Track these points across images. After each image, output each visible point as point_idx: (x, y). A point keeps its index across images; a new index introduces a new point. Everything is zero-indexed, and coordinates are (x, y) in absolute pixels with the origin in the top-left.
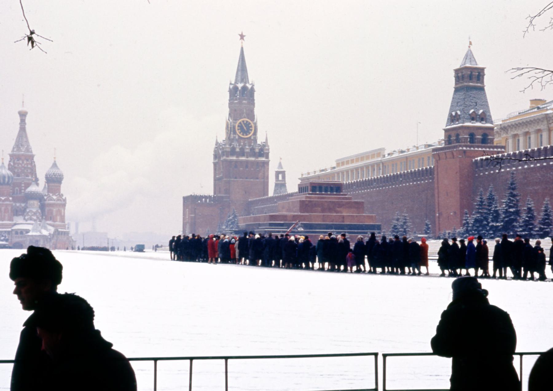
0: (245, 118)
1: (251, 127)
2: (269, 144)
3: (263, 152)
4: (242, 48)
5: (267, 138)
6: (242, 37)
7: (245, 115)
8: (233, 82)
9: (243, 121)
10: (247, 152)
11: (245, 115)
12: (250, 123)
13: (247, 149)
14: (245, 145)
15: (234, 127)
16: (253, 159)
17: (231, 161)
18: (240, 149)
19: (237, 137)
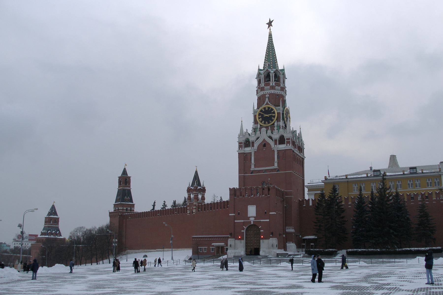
5: (300, 132)
6: (270, 24)
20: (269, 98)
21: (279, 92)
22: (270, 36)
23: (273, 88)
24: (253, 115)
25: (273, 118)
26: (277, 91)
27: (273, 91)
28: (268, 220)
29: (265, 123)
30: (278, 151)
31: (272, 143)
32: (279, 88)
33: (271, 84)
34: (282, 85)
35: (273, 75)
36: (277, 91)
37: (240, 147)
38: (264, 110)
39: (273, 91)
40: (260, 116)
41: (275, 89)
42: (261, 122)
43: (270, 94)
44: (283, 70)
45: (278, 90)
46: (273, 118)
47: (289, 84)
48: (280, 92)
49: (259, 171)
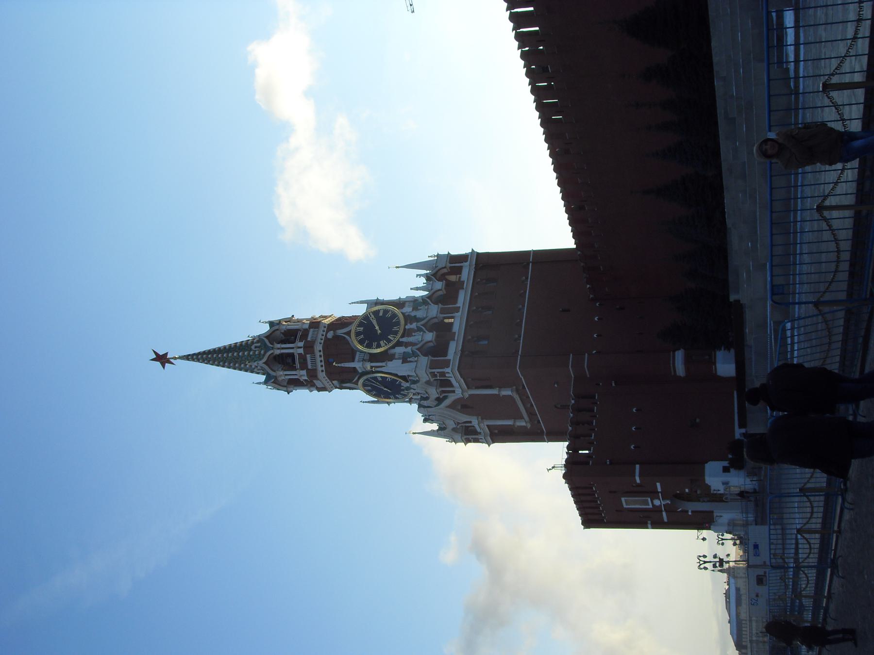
0: (348, 334)
1: (376, 313)
2: (425, 256)
3: (446, 272)
4: (188, 357)
6: (162, 359)
7: (340, 332)
8: (263, 378)
9: (358, 334)
10: (442, 311)
11: (340, 332)
12: (366, 317)
13: (434, 310)
14: (416, 319)
15: (373, 358)
16: (463, 298)
17: (465, 353)
18: (430, 331)
19: (399, 350)
21: (318, 359)
22: (188, 357)
23: (313, 374)
26: (319, 364)
28: (658, 485)
30: (468, 388)
31: (452, 398)
32: (308, 356)
34: (301, 351)
35: (281, 373)
36: (319, 361)
37: (476, 441)
39: (322, 375)
42: (405, 395)
43: (331, 379)
45: (314, 362)
48: (318, 354)
49: (531, 414)
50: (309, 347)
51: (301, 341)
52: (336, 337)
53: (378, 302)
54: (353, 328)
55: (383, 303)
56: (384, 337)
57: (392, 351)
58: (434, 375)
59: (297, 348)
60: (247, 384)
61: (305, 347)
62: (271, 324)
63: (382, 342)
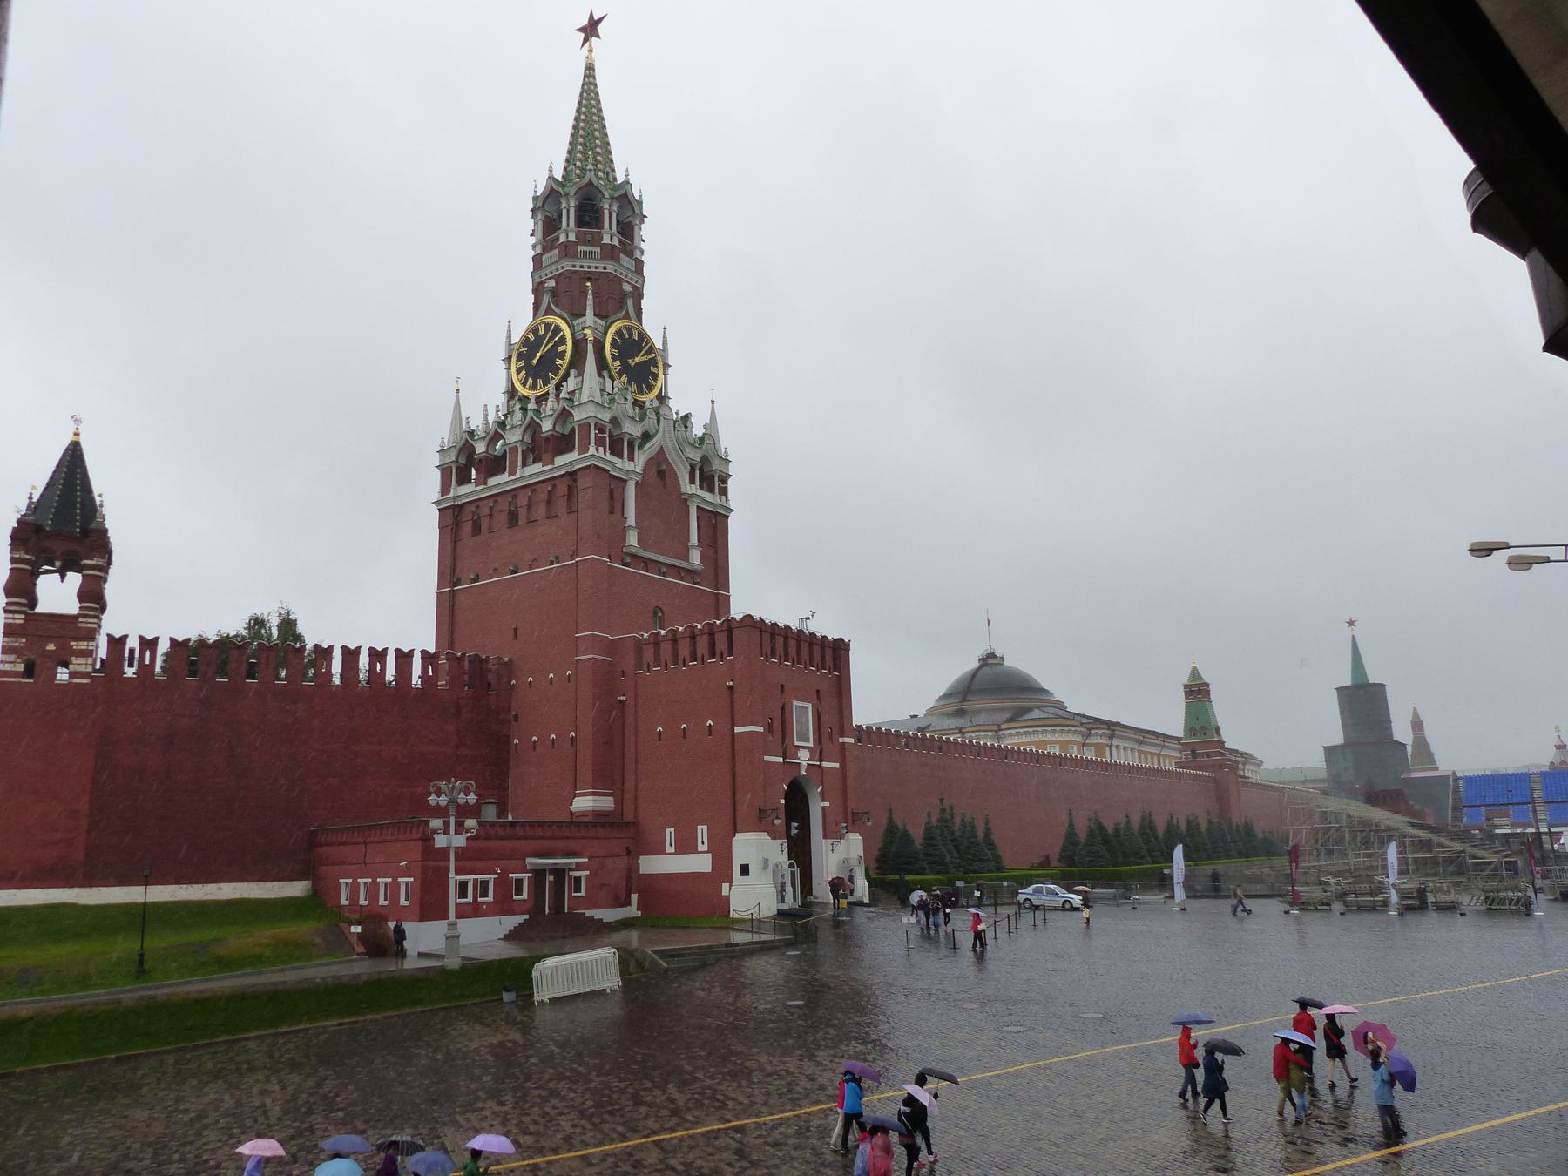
0: (627, 316)
1: (654, 362)
2: (727, 441)
4: (590, 69)
6: (591, 29)
7: (630, 303)
9: (629, 329)
20: (554, 293)
21: (593, 265)
23: (568, 250)
24: (504, 365)
25: (559, 362)
27: (567, 265)
29: (535, 387)
33: (562, 239)
34: (606, 240)
36: (589, 262)
38: (532, 338)
39: (567, 265)
40: (522, 363)
41: (576, 256)
42: (524, 384)
43: (557, 278)
44: (627, 182)
45: (589, 256)
46: (559, 362)
47: (652, 237)
50: (611, 253)
51: (621, 242)
52: (624, 295)
53: (666, 366)
54: (634, 323)
55: (665, 374)
56: (625, 369)
57: (605, 373)
58: (585, 427)
59: (609, 236)
60: (549, 155)
61: (613, 246)
62: (640, 203)
63: (618, 363)
